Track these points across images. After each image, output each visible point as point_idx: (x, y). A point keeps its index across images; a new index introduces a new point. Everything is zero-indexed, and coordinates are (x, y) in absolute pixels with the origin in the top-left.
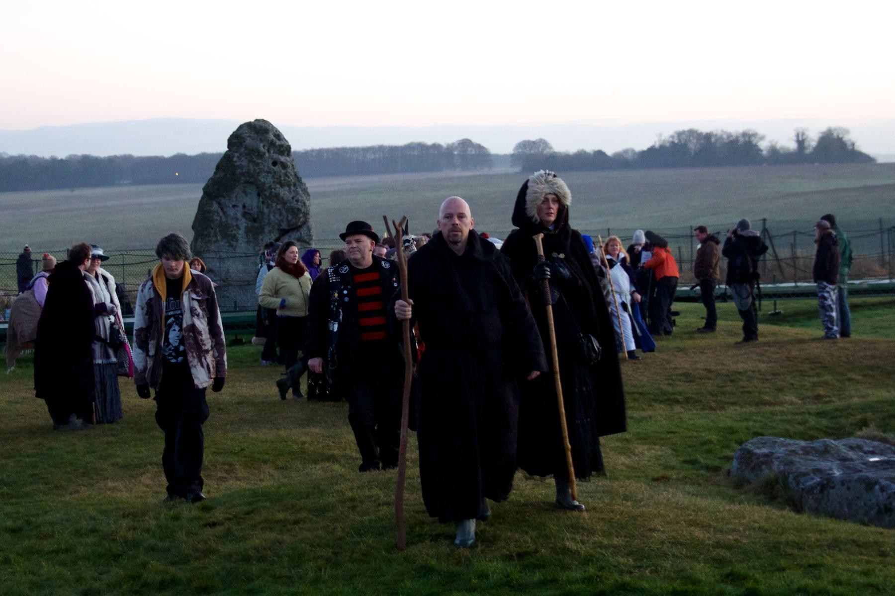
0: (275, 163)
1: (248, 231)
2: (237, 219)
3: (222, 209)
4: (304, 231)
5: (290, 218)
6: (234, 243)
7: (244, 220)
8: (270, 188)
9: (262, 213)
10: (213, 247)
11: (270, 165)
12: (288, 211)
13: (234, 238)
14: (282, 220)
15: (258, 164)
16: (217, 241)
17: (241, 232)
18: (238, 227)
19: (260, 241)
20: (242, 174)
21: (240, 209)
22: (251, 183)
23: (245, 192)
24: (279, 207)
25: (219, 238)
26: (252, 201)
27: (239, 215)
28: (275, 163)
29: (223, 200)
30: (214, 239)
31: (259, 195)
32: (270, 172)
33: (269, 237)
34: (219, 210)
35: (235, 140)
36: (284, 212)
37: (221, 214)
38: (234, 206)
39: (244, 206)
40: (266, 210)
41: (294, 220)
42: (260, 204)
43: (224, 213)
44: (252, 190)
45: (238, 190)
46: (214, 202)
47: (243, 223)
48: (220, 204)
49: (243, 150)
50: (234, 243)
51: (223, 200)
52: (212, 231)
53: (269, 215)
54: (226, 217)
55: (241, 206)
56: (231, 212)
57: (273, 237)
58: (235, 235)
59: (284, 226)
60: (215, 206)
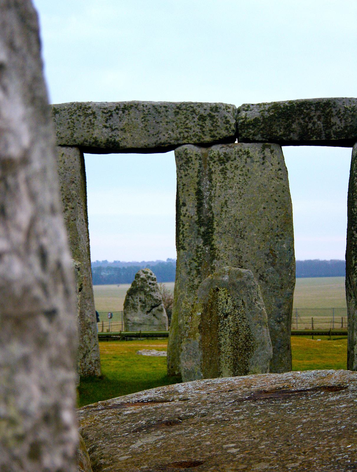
0: (150, 284)
1: (141, 306)
6: (136, 310)
8: (148, 292)
10: (130, 312)
13: (137, 309)
17: (139, 307)
18: (138, 305)
20: (139, 287)
21: (138, 300)
22: (142, 290)
23: (140, 293)
26: (142, 296)
29: (133, 296)
31: (145, 294)
33: (148, 309)
39: (140, 298)
40: (147, 300)
43: (133, 300)
45: (138, 293)
47: (140, 304)
48: (132, 297)
49: (139, 279)
50: (136, 310)
55: (139, 298)
56: (136, 300)
57: (149, 308)
59: (153, 305)
60: (130, 298)
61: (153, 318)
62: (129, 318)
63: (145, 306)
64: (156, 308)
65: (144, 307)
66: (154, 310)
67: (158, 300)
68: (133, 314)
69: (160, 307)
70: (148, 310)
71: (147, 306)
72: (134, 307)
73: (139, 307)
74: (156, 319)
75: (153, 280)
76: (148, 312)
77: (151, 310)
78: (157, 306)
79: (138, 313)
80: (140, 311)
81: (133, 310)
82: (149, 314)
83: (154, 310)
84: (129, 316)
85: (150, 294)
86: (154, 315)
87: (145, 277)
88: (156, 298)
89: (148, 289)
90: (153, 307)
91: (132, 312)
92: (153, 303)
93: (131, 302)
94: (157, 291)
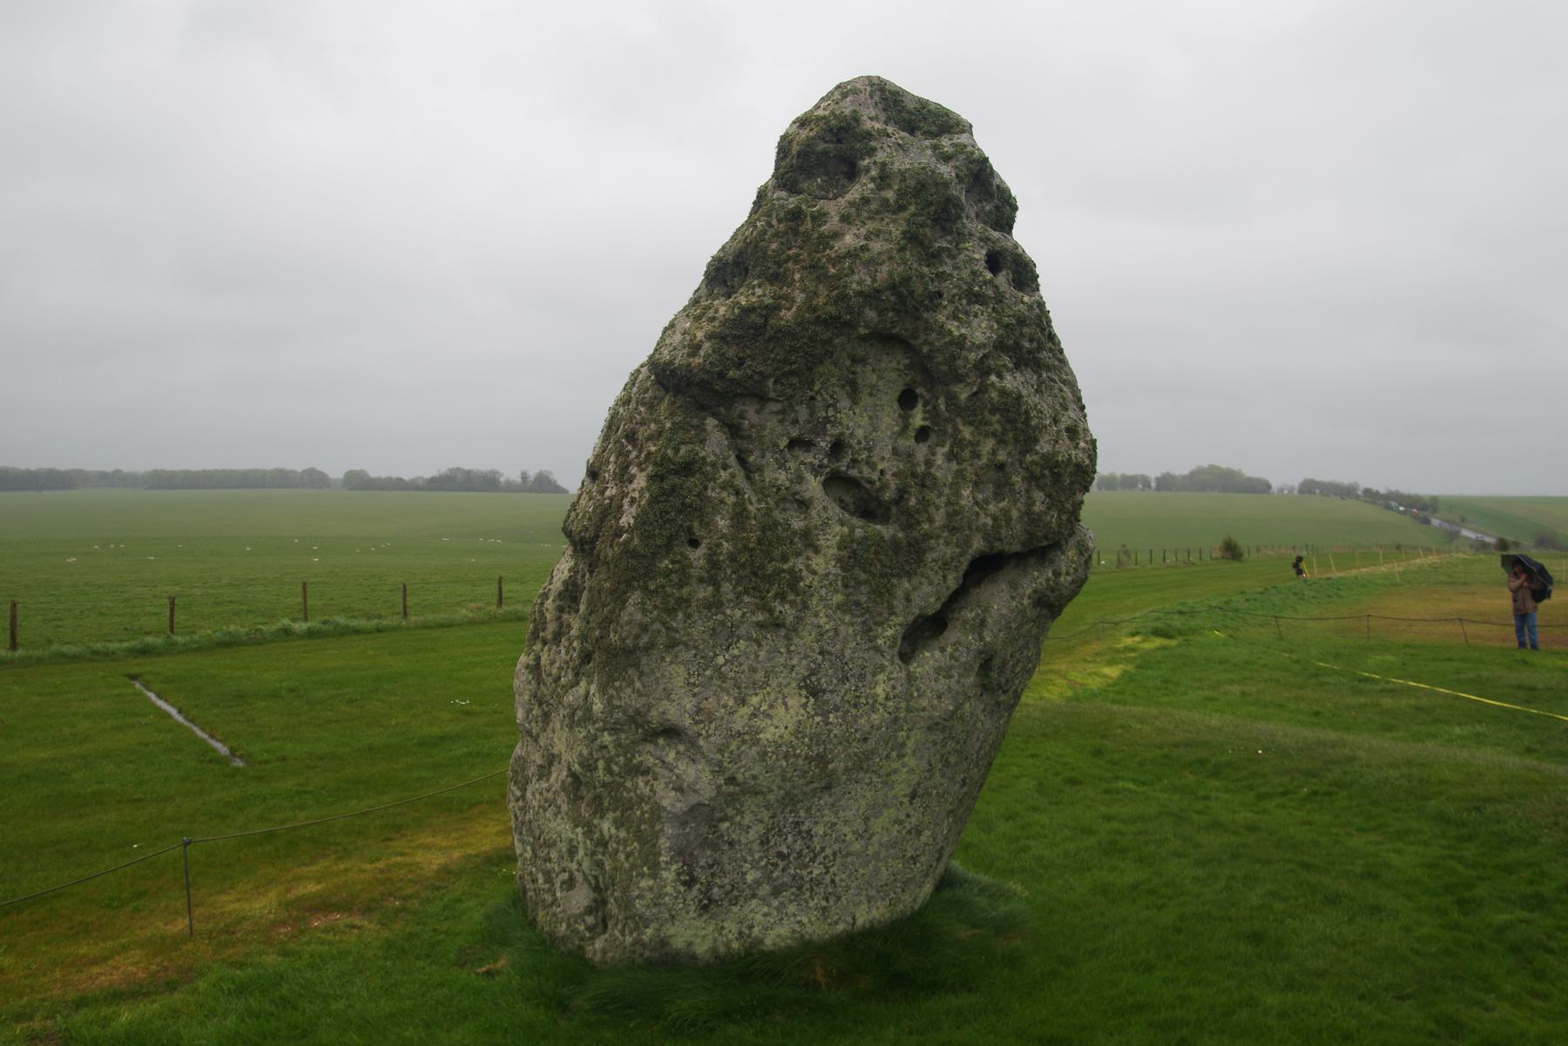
1: (853, 557)
2: (804, 505)
3: (742, 460)
4: (1067, 559)
5: (1038, 507)
7: (835, 511)
8: (982, 368)
9: (926, 482)
11: (981, 266)
12: (1032, 479)
14: (1006, 513)
15: (933, 257)
17: (823, 562)
18: (808, 540)
19: (899, 604)
20: (871, 297)
22: (885, 339)
24: (1002, 456)
25: (726, 587)
26: (874, 426)
27: (813, 486)
28: (995, 261)
30: (705, 592)
31: (907, 400)
32: (979, 299)
33: (926, 593)
34: (732, 460)
35: (826, 151)
37: (740, 481)
39: (838, 447)
40: (943, 469)
42: (907, 443)
44: (886, 374)
46: (711, 422)
48: (733, 430)
50: (787, 612)
51: (750, 414)
52: (697, 556)
53: (955, 488)
54: (762, 493)
57: (953, 582)
58: (795, 578)
60: (715, 443)
62: (678, 709)
66: (1000, 601)
70: (934, 606)
72: (763, 569)
76: (928, 628)
84: (675, 693)
87: (946, 170)
89: (980, 330)
90: (985, 567)
92: (991, 514)
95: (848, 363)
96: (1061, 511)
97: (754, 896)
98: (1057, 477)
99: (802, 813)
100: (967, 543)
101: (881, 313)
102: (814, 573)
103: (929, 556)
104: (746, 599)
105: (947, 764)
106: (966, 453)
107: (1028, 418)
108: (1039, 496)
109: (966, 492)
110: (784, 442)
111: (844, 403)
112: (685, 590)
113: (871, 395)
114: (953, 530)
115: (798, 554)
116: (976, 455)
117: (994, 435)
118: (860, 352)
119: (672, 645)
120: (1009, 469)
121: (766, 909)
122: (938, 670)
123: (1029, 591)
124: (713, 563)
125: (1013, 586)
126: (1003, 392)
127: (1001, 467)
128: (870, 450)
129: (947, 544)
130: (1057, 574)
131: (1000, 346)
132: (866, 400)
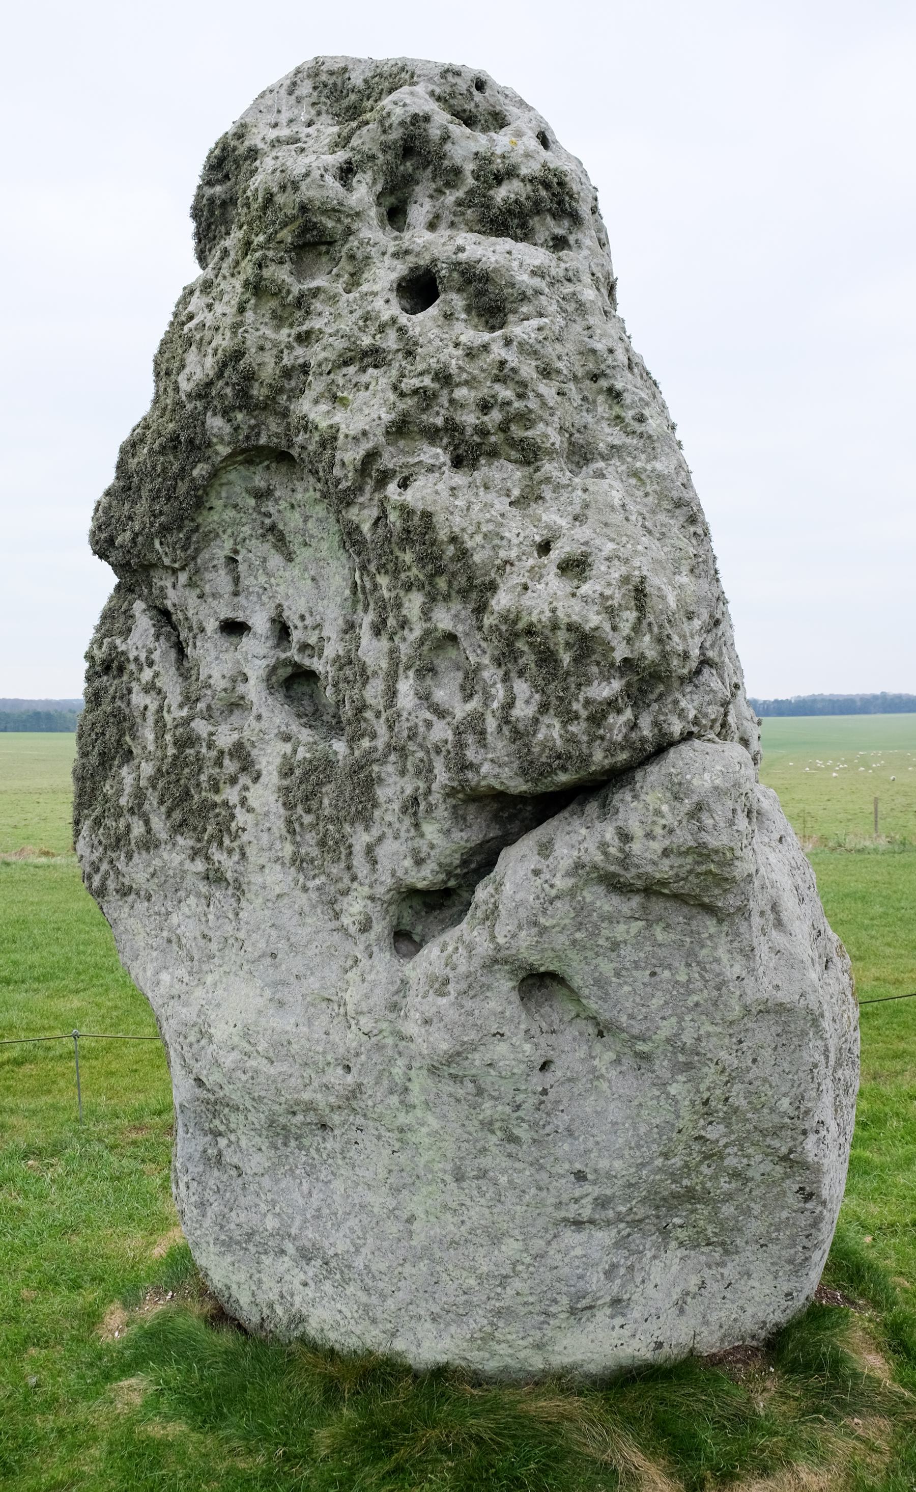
0: (419, 289)
1: (304, 786)
5: (523, 711)
12: (506, 657)
14: (474, 725)
16: (149, 844)
17: (265, 795)
21: (256, 654)
24: (444, 619)
36: (479, 653)
38: (234, 628)
39: (282, 631)
40: (373, 651)
41: (551, 731)
48: (164, 617)
54: (189, 700)
55: (260, 622)
57: (443, 840)
59: (496, 768)
61: (512, 1039)
63: (363, 783)
64: (575, 840)
65: (331, 801)
67: (586, 643)
68: (185, 919)
69: (644, 817)
71: (393, 788)
72: (193, 802)
73: (261, 801)
74: (573, 1050)
75: (507, 223)
77: (481, 863)
78: (594, 789)
79: (253, 910)
80: (277, 878)
81: (175, 856)
82: (432, 955)
83: (522, 873)
85: (419, 529)
86: (539, 983)
88: (544, 597)
90: (519, 812)
91: (174, 887)
93: (157, 692)
94: (580, 454)
95: (252, 502)
96: (569, 717)
97: (283, 1252)
98: (547, 657)
99: (313, 1152)
100: (425, 771)
101: (226, 413)
102: (250, 810)
103: (382, 793)
104: (180, 840)
105: (513, 1139)
106: (391, 622)
107: (463, 554)
108: (521, 688)
109: (406, 686)
110: (211, 625)
111: (276, 560)
112: (122, 823)
113: (306, 544)
114: (402, 751)
115: (233, 780)
116: (404, 624)
117: (421, 587)
118: (259, 481)
119: (125, 892)
120: (464, 643)
121: (302, 1276)
122: (432, 980)
123: (566, 864)
124: (139, 795)
125: (545, 849)
126: (406, 512)
127: (452, 638)
128: (318, 626)
129: (403, 773)
130: (625, 837)
131: (400, 429)
132: (303, 555)
